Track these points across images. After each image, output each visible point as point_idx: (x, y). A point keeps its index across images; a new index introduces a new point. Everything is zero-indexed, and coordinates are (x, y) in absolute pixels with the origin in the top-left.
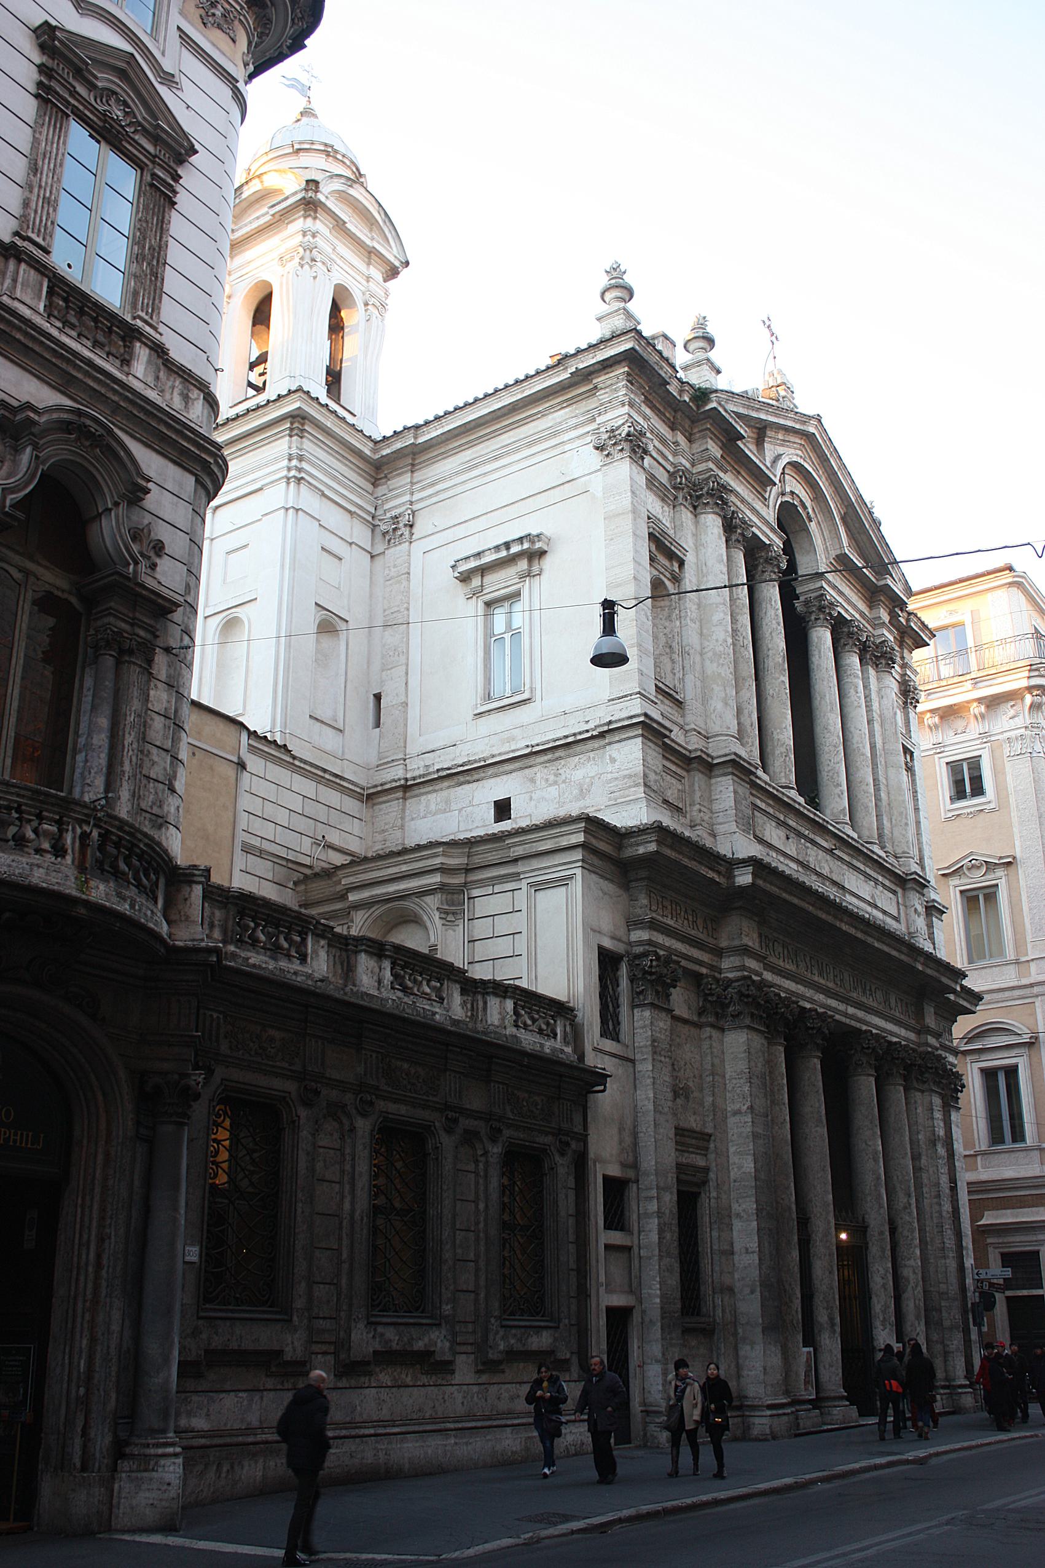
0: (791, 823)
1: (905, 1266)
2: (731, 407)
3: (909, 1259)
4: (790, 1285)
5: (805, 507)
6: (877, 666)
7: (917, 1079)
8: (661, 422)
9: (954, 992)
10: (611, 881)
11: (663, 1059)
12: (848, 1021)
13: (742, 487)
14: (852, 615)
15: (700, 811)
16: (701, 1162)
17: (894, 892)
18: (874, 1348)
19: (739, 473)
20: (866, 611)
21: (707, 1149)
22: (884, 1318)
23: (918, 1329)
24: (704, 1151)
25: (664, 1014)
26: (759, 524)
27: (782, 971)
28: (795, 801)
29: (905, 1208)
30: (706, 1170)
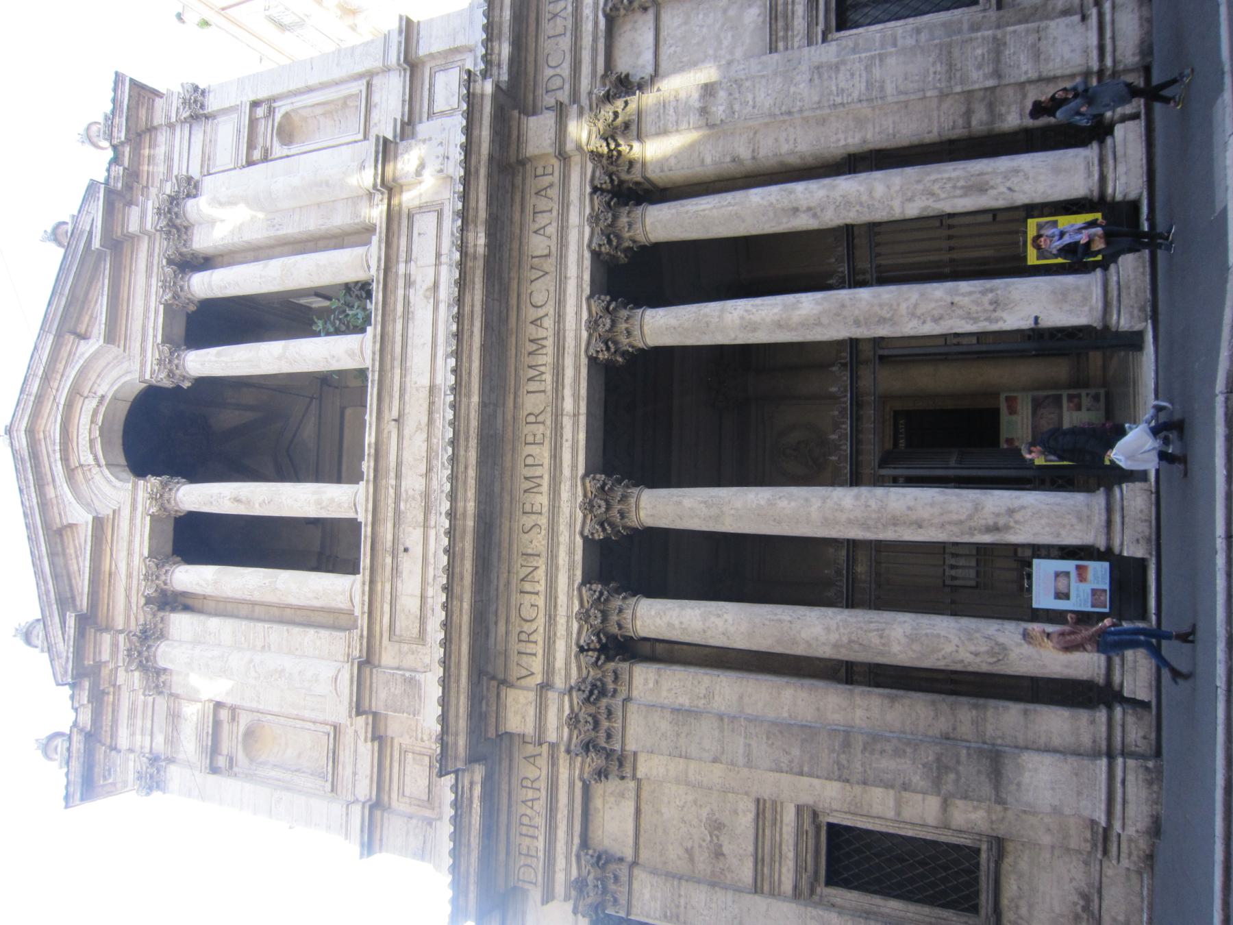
0: (389, 537)
1: (903, 212)
2: (61, 647)
3: (891, 208)
4: (938, 660)
5: (95, 413)
6: (186, 228)
7: (629, 172)
8: (122, 699)
9: (497, 86)
10: (524, 913)
11: (682, 901)
12: (583, 409)
13: (121, 524)
14: (143, 518)
15: (422, 740)
16: (789, 816)
17: (410, 217)
18: (1032, 330)
19: (110, 574)
20: (144, 246)
21: (774, 803)
22: (986, 320)
23: (1002, 189)
24: (776, 806)
25: (636, 885)
26: (151, 338)
27: (550, 617)
28: (375, 336)
29: (815, 216)
30: (799, 809)
